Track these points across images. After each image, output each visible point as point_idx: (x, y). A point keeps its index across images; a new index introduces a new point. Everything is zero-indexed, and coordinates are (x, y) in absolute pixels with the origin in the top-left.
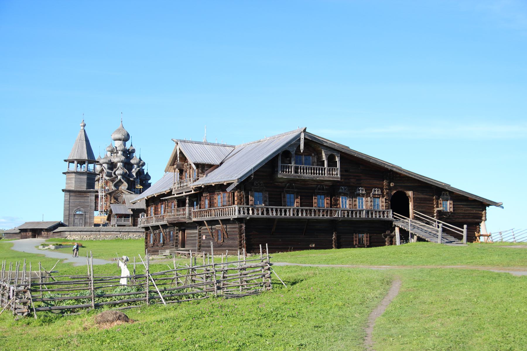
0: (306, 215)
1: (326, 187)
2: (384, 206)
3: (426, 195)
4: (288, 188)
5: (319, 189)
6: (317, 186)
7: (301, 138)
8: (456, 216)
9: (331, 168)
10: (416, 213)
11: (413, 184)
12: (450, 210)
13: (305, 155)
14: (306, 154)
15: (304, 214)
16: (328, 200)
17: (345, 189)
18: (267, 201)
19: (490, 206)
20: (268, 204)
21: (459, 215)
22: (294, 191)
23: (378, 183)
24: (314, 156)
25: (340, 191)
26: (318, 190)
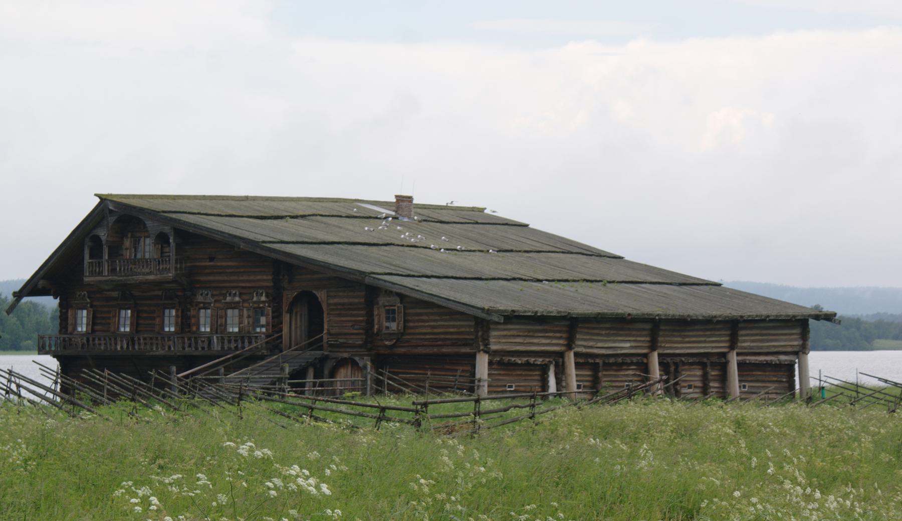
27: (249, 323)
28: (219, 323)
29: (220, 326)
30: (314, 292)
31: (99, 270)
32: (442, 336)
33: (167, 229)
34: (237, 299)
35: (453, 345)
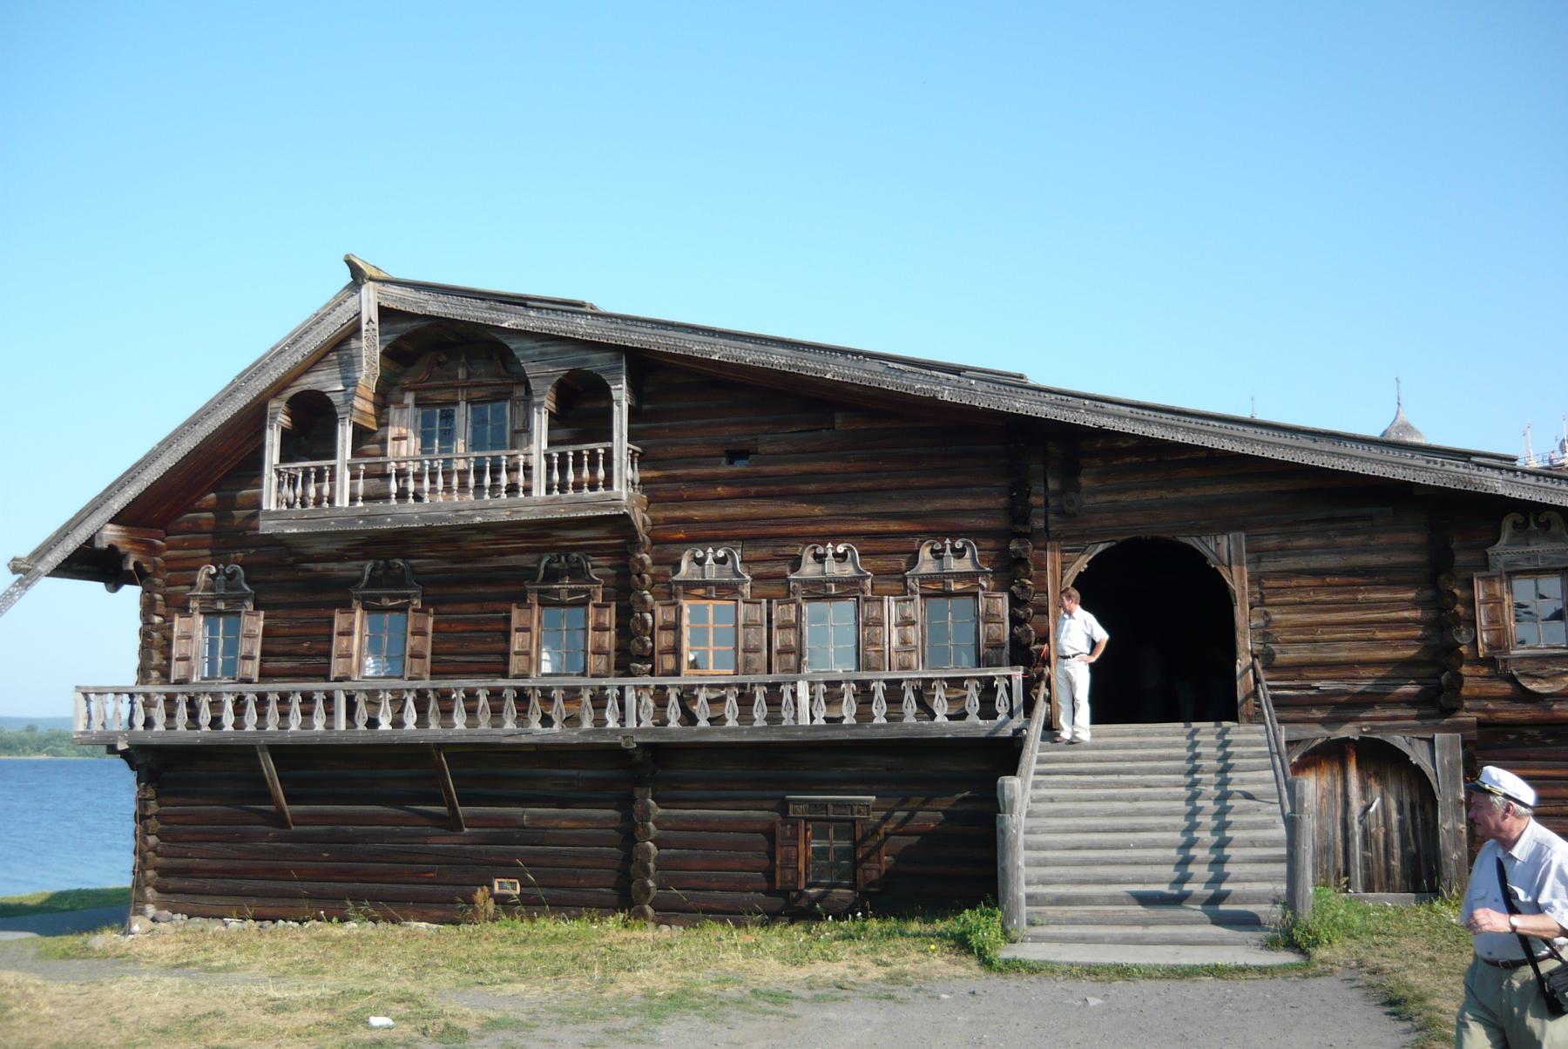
0: (422, 722)
4: (374, 582)
6: (540, 560)
7: (364, 320)
9: (585, 448)
14: (476, 394)
15: (411, 717)
23: (966, 503)
27: (904, 642)
28: (777, 644)
29: (779, 652)
30: (1193, 542)
31: (319, 491)
33: (596, 362)
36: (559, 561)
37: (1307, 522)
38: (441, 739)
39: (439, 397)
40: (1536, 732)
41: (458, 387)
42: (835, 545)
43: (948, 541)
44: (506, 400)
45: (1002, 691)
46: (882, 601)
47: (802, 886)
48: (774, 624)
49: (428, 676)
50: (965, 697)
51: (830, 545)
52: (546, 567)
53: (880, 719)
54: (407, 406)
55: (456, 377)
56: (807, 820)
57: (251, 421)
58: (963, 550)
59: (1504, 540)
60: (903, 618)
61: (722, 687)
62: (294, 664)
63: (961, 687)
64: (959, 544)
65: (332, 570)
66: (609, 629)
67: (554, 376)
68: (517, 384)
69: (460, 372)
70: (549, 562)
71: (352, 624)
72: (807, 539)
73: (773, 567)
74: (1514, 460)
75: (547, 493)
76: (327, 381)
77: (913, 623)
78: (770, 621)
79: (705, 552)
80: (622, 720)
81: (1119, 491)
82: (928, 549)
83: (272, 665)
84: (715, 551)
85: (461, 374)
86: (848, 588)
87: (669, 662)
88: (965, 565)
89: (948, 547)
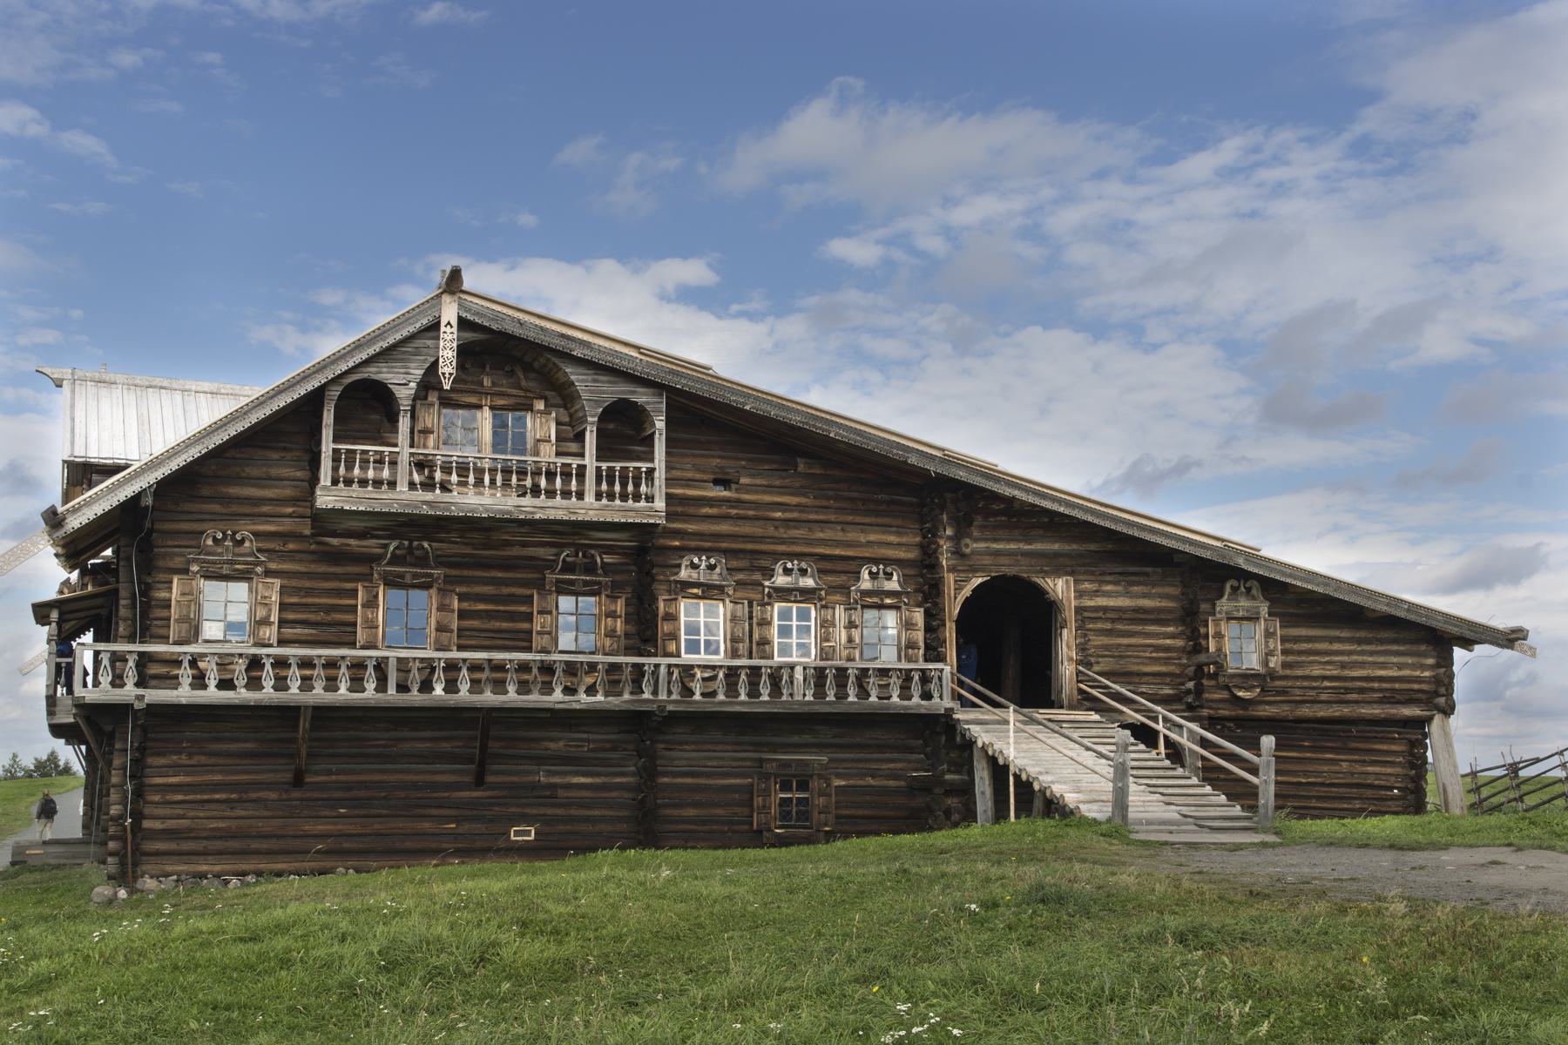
1: (608, 559)
2: (922, 644)
3: (1144, 596)
5: (568, 568)
6: (558, 555)
8: (1298, 692)
10: (961, 684)
11: (1075, 547)
12: (1266, 663)
13: (492, 408)
14: (501, 402)
16: (612, 615)
17: (711, 568)
18: (270, 624)
19: (1477, 648)
20: (274, 640)
21: (1314, 688)
22: (431, 575)
23: (892, 539)
24: (546, 412)
25: (684, 574)
26: (563, 571)
27: (850, 640)
28: (756, 636)
29: (758, 644)
30: (1040, 581)
32: (1359, 684)
33: (642, 397)
34: (809, 582)
35: (1381, 701)
36: (577, 555)
37: (1110, 574)
38: (275, 702)
39: (463, 399)
40: (1232, 725)
41: (482, 393)
42: (885, 565)
43: (881, 567)
44: (527, 410)
45: (935, 680)
46: (834, 608)
47: (773, 826)
48: (755, 620)
49: (455, 648)
50: (889, 684)
51: (796, 562)
52: (564, 559)
53: (831, 697)
54: (432, 405)
55: (482, 384)
56: (776, 776)
57: (314, 401)
58: (892, 574)
59: (1226, 597)
60: (850, 622)
61: (713, 668)
62: (314, 632)
63: (888, 676)
64: (889, 570)
65: (349, 545)
66: (620, 617)
67: (604, 402)
68: (536, 398)
69: (485, 380)
70: (567, 555)
71: (376, 596)
72: (776, 557)
73: (750, 575)
74: (1259, 550)
75: (596, 500)
76: (387, 374)
77: (856, 627)
78: (751, 618)
79: (700, 560)
80: (655, 692)
81: (996, 540)
82: (867, 572)
83: (288, 631)
84: (708, 558)
85: (487, 382)
86: (807, 595)
87: (672, 647)
88: (893, 585)
89: (881, 571)
